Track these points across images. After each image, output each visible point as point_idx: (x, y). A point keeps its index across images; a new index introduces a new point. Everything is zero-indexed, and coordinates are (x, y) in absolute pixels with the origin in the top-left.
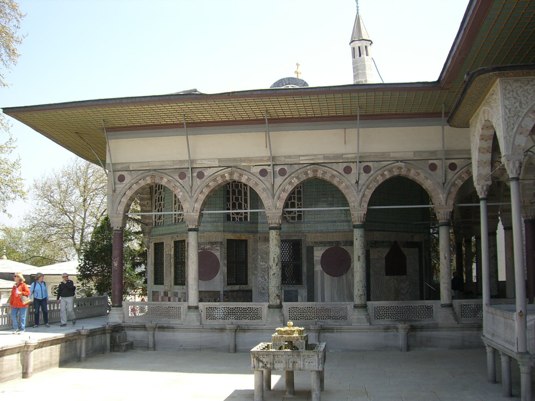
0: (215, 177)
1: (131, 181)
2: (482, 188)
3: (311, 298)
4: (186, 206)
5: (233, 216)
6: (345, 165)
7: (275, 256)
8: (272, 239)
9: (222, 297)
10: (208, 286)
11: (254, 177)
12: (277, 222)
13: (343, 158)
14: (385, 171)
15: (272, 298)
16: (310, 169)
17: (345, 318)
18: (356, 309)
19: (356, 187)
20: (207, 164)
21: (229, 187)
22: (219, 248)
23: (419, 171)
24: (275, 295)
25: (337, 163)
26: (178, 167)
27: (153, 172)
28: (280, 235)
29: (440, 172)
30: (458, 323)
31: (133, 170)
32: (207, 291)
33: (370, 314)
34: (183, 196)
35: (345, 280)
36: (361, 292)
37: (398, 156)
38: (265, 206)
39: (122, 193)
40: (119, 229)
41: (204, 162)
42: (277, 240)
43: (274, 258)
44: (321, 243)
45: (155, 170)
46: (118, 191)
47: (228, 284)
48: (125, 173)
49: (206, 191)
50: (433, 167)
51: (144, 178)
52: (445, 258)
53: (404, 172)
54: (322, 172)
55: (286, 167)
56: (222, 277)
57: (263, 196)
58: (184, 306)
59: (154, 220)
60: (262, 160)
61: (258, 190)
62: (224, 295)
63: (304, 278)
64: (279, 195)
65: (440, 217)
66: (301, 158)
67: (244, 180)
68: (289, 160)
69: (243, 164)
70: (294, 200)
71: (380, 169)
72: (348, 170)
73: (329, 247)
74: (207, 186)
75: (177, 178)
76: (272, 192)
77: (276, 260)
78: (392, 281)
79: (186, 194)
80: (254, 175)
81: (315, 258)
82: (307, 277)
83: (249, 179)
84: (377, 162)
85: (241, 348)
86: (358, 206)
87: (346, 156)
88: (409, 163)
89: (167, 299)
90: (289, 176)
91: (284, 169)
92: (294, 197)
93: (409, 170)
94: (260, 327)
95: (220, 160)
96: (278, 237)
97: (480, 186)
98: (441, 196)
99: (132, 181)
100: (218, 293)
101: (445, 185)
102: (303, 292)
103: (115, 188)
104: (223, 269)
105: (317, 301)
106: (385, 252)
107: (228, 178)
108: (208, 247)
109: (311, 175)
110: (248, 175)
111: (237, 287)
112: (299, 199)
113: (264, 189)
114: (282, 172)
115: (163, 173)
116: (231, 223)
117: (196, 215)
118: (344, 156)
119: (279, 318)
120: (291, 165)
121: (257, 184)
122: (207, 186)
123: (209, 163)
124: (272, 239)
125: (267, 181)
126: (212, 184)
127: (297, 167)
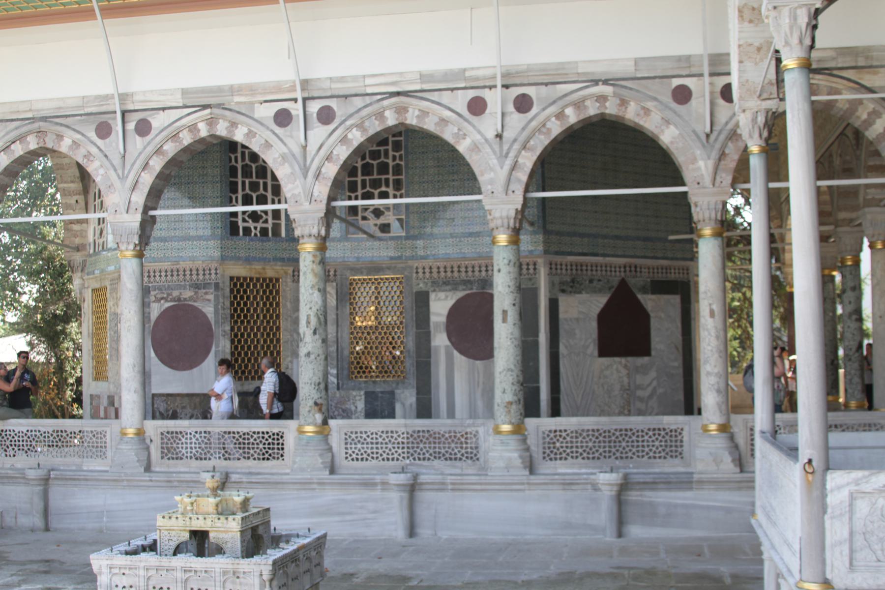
2: (754, 120)
3: (424, 410)
4: (113, 199)
5: (246, 225)
6: (472, 94)
7: (310, 312)
12: (315, 231)
13: (466, 79)
14: (566, 106)
16: (389, 107)
17: (473, 456)
19: (496, 148)
21: (236, 158)
23: (650, 105)
24: (311, 403)
25: (452, 90)
27: (41, 124)
29: (700, 105)
30: (742, 471)
32: (188, 395)
33: (533, 448)
34: (106, 177)
36: (509, 397)
37: (599, 70)
38: (288, 195)
42: (315, 275)
43: (308, 316)
45: (44, 119)
49: (157, 164)
52: (712, 314)
53: (611, 108)
55: (333, 104)
57: (282, 172)
58: (111, 428)
61: (271, 158)
65: (701, 218)
66: (368, 81)
67: (239, 136)
69: (237, 99)
70: (387, 185)
71: (554, 102)
72: (477, 107)
75: (93, 135)
77: (314, 321)
78: (616, 367)
81: (433, 319)
83: (250, 134)
84: (546, 84)
86: (501, 189)
88: (626, 87)
89: (113, 415)
90: (340, 124)
92: (387, 180)
93: (624, 103)
95: (185, 92)
96: (318, 269)
97: (749, 115)
98: (701, 164)
101: (712, 137)
105: (438, 417)
106: (592, 304)
107: (204, 131)
108: (188, 294)
109: (391, 120)
110: (247, 125)
112: (398, 185)
114: (326, 116)
115: (61, 125)
116: (241, 241)
117: (135, 219)
119: (321, 455)
120: (346, 97)
121: (268, 145)
124: (305, 273)
125: (291, 136)
126: (171, 149)
127: (358, 102)
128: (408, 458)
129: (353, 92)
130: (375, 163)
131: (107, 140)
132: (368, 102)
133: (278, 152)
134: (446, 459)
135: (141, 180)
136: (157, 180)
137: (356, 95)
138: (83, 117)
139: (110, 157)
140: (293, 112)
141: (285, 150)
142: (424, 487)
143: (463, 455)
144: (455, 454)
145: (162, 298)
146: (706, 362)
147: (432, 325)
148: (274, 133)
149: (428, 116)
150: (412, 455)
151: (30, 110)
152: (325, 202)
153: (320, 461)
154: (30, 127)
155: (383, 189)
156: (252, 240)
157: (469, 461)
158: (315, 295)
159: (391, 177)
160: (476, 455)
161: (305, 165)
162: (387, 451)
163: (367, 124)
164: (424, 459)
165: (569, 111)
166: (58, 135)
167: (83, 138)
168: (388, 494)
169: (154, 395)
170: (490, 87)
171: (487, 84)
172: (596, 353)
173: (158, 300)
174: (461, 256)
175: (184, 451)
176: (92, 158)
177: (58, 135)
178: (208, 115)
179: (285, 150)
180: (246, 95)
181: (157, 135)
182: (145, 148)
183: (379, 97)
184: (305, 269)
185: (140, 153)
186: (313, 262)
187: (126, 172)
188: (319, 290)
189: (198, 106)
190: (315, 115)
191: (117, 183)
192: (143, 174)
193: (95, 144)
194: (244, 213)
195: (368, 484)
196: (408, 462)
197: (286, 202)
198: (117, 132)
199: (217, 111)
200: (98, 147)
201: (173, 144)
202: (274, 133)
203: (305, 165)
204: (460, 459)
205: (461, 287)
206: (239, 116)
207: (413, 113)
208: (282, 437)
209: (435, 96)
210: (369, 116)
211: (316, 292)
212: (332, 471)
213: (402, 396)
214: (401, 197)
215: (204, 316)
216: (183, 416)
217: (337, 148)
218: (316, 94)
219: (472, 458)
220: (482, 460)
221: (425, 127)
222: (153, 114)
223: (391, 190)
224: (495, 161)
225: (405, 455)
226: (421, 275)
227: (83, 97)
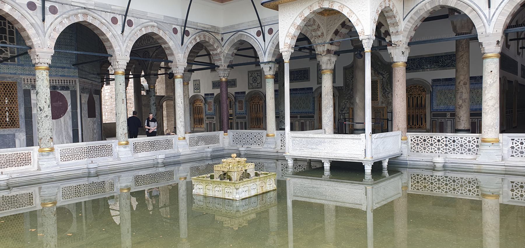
6: (113, 15)
8: (42, 80)
19: (121, 38)
24: (49, 137)
25: (106, 12)
35: (63, 123)
36: (126, 131)
50: (175, 31)
53: (155, 31)
55: (57, 5)
70: (6, 40)
77: (48, 102)
80: (21, 7)
92: (5, 37)
102: (21, 136)
109: (81, 19)
113: (32, 24)
124: (42, 80)
141: (34, 22)
146: (180, 118)
165: (143, 29)
172: (87, 115)
202: (27, 12)
209: (99, 13)
224: (121, 43)
226: (26, 82)
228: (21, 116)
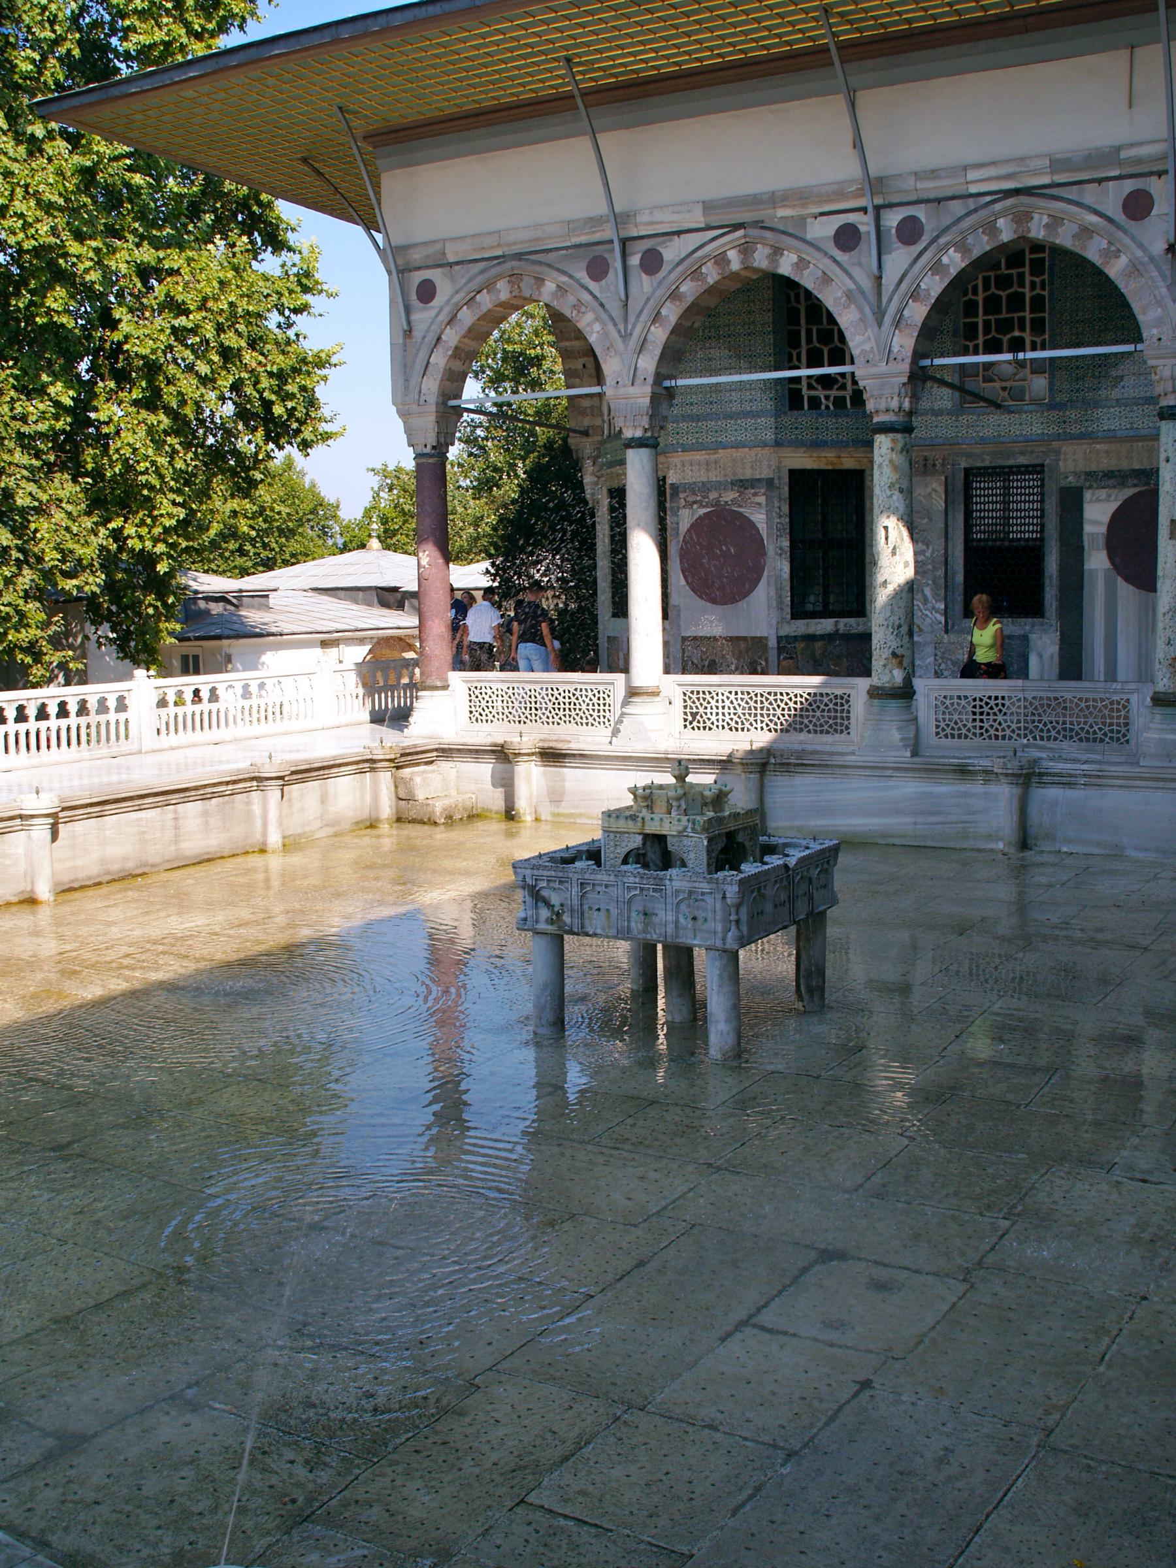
0: (700, 261)
1: (452, 296)
5: (813, 393)
6: (1129, 186)
9: (773, 655)
10: (711, 623)
11: (817, 254)
12: (894, 404)
15: (877, 664)
18: (1157, 710)
20: (668, 220)
22: (762, 499)
24: (886, 653)
26: (583, 239)
27: (514, 263)
28: (906, 450)
31: (457, 263)
34: (605, 334)
38: (856, 352)
39: (431, 338)
40: (428, 450)
41: (659, 216)
42: (895, 468)
44: (1109, 475)
45: (518, 256)
46: (418, 333)
47: (795, 616)
48: (434, 275)
49: (672, 313)
51: (489, 286)
54: (1045, 220)
55: (920, 212)
56: (773, 593)
57: (847, 319)
59: (606, 418)
60: (840, 195)
61: (830, 299)
62: (780, 649)
63: (1051, 595)
64: (900, 311)
66: (972, 175)
68: (931, 184)
69: (781, 213)
70: (1022, 328)
73: (1138, 489)
74: (674, 295)
75: (583, 276)
76: (875, 304)
79: (611, 327)
80: (818, 249)
81: (1088, 529)
82: (1061, 590)
83: (801, 264)
85: (781, 824)
87: (1133, 152)
91: (913, 220)
92: (1022, 321)
94: (837, 760)
95: (708, 206)
96: (899, 459)
99: (456, 299)
100: (758, 643)
102: (1045, 645)
103: (409, 322)
104: (778, 567)
107: (735, 261)
108: (729, 496)
109: (1006, 232)
110: (797, 251)
111: (825, 625)
112: (1038, 326)
113: (849, 295)
114: (910, 231)
115: (540, 263)
116: (805, 418)
117: (642, 395)
118: (1124, 154)
120: (939, 201)
121: (826, 279)
122: (674, 295)
123: (675, 217)
124: (880, 466)
125: (860, 265)
126: (689, 289)
128: (1025, 736)
129: (950, 194)
130: (1003, 294)
131: (603, 283)
132: (972, 207)
133: (839, 292)
134: (1081, 740)
135: (650, 337)
136: (673, 337)
137: (953, 198)
138: (570, 251)
139: (607, 306)
140: (863, 229)
141: (852, 286)
142: (1045, 779)
143: (1105, 734)
144: (1095, 733)
145: (695, 502)
147: (1085, 538)
148: (835, 261)
149: (1062, 224)
150: (1031, 732)
151: (499, 245)
152: (908, 360)
153: (899, 737)
154: (499, 269)
155: (1017, 333)
156: (821, 415)
157: (1115, 744)
158: (895, 498)
159: (1028, 315)
160: (1124, 735)
161: (879, 307)
162: (996, 725)
163: (970, 240)
164: (1049, 738)
166: (537, 279)
167: (571, 281)
168: (992, 788)
169: (684, 639)
170: (1160, 174)
171: (1155, 169)
173: (689, 505)
174: (1131, 433)
175: (714, 718)
176: (583, 309)
177: (537, 279)
178: (740, 238)
179: (852, 286)
180: (794, 206)
181: (670, 272)
182: (654, 291)
183: (988, 198)
184: (881, 460)
185: (648, 299)
186: (892, 449)
187: (630, 327)
188: (901, 491)
189: (727, 226)
190: (894, 231)
191: (619, 342)
192: (652, 328)
193: (587, 289)
194: (809, 377)
195: (963, 772)
196: (1025, 741)
197: (853, 363)
198: (616, 269)
199: (754, 232)
200: (591, 293)
201: (694, 284)
202: (835, 261)
203: (879, 307)
204: (1102, 741)
205: (1130, 482)
206: (784, 237)
207: (1041, 219)
208: (848, 702)
209: (1072, 193)
210: (974, 229)
211: (897, 493)
212: (915, 753)
213: (1039, 643)
214: (1043, 348)
215: (753, 526)
216: (723, 668)
217: (926, 279)
218: (895, 200)
219: (1118, 739)
220: (1132, 742)
221: (1057, 241)
222: (664, 242)
223: (1027, 337)
224: (1164, 291)
225: (1022, 732)
227: (569, 222)
228: (1051, 577)
